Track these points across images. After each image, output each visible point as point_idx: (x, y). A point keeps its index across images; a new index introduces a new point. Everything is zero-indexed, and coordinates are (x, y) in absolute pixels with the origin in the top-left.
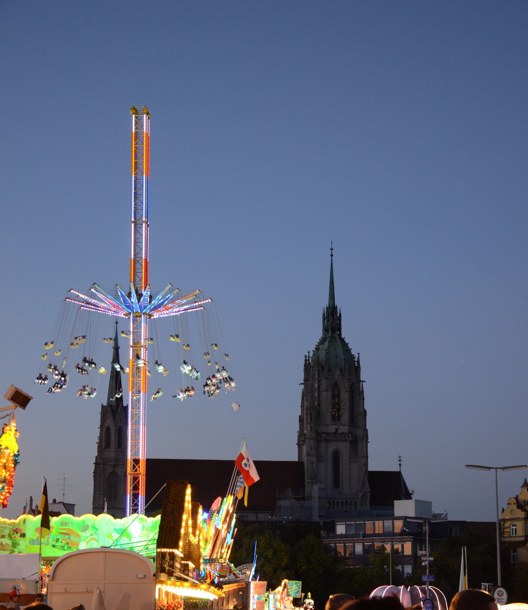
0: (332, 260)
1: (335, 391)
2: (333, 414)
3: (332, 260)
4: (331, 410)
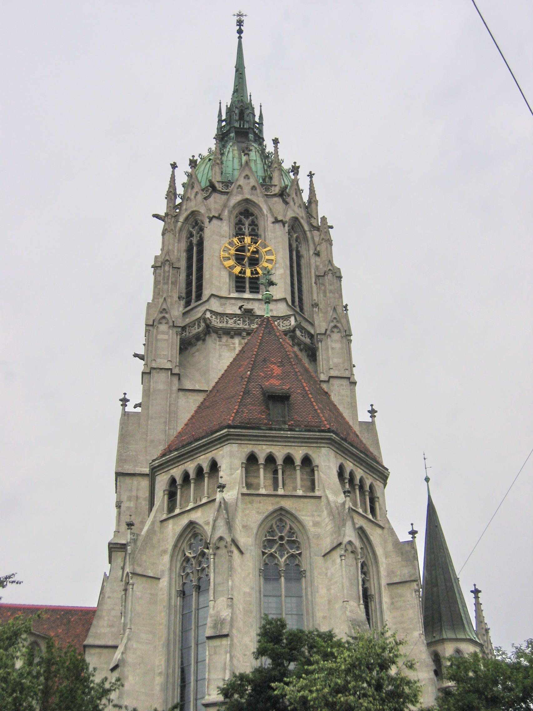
0: (240, 38)
1: (244, 225)
2: (237, 269)
3: (240, 38)
4: (231, 262)
